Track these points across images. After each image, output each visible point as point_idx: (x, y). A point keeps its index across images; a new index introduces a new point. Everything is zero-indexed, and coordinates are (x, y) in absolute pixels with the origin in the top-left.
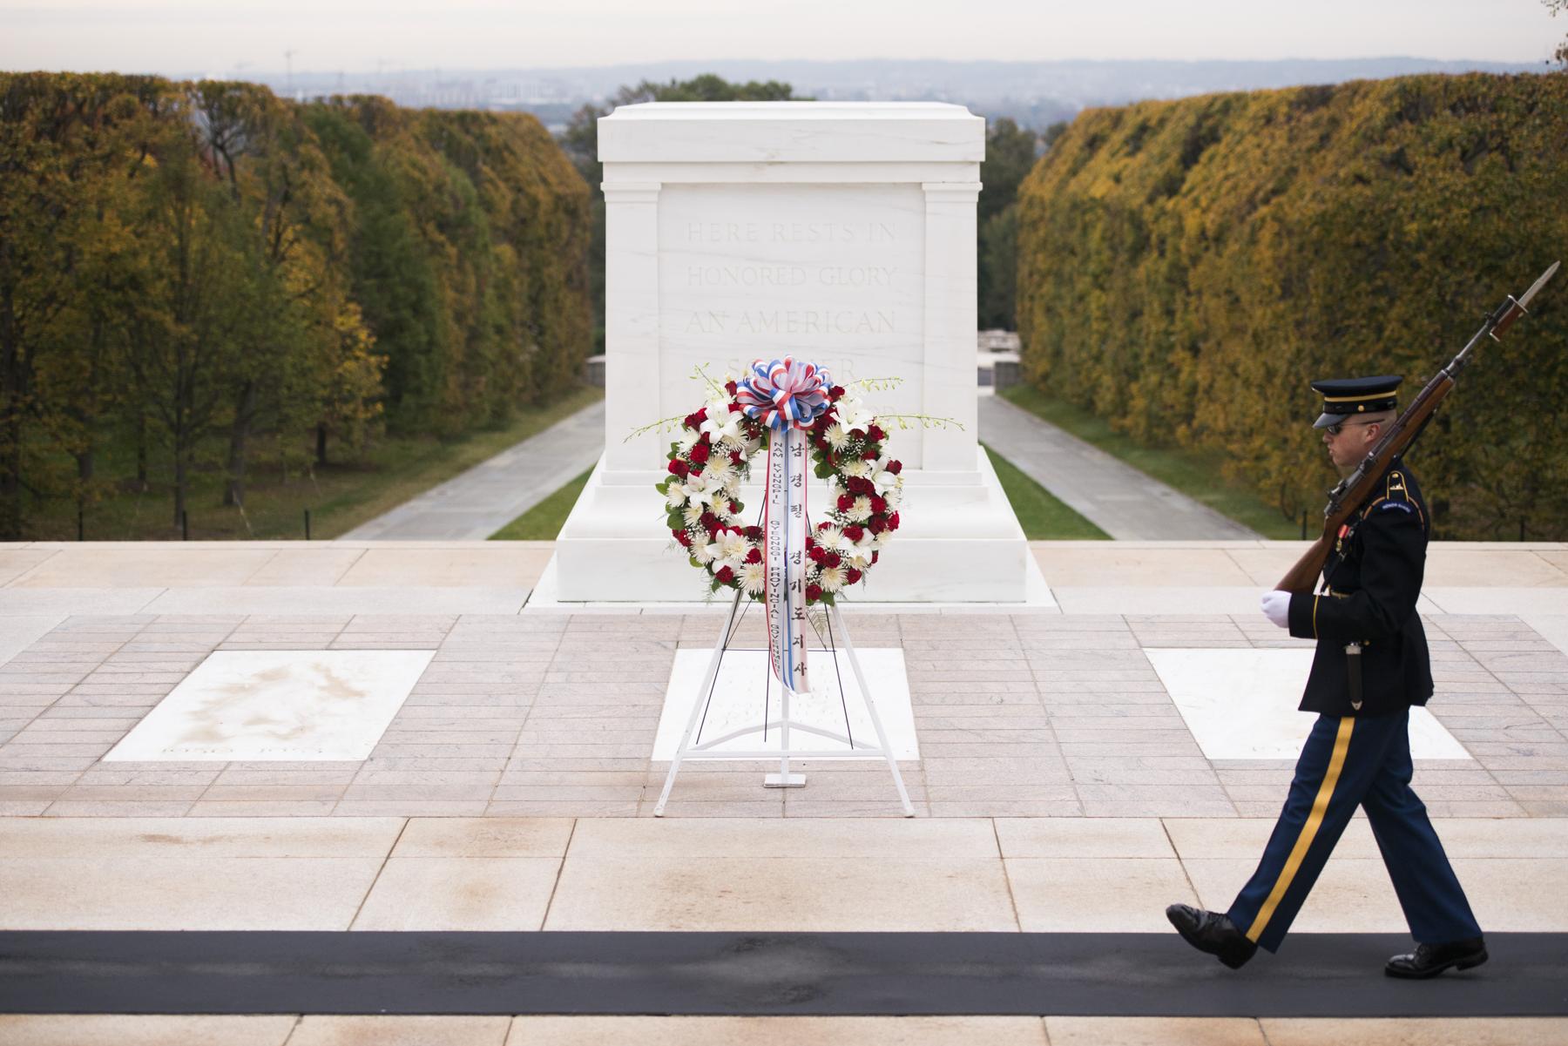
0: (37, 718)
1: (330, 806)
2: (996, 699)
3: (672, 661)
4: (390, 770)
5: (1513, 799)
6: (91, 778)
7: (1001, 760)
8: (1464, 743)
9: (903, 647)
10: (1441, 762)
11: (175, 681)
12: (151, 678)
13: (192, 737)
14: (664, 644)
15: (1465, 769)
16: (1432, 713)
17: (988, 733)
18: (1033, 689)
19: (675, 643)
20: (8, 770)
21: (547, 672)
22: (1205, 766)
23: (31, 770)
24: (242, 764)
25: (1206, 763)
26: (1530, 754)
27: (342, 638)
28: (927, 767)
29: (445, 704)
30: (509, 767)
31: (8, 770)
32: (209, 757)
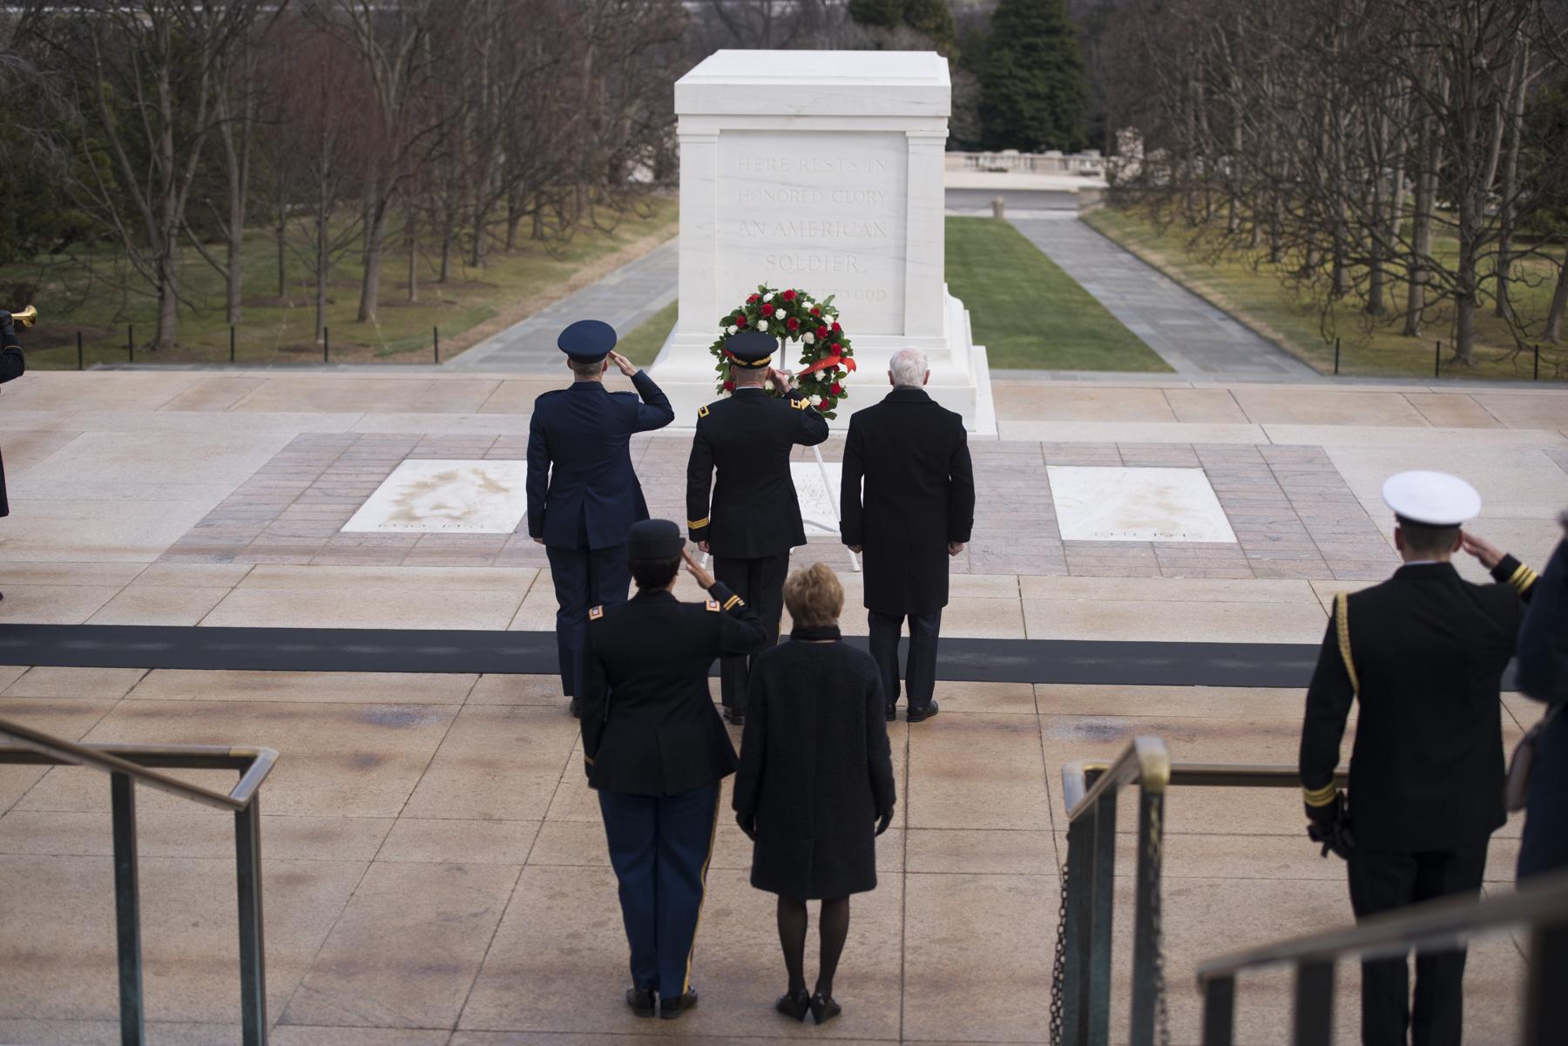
5: (1252, 568)
6: (335, 542)
10: (1216, 544)
11: (380, 479)
12: (364, 478)
13: (397, 517)
15: (1229, 547)
16: (1225, 512)
20: (280, 536)
22: (1059, 544)
24: (432, 534)
26: (1278, 539)
27: (491, 451)
31: (280, 536)
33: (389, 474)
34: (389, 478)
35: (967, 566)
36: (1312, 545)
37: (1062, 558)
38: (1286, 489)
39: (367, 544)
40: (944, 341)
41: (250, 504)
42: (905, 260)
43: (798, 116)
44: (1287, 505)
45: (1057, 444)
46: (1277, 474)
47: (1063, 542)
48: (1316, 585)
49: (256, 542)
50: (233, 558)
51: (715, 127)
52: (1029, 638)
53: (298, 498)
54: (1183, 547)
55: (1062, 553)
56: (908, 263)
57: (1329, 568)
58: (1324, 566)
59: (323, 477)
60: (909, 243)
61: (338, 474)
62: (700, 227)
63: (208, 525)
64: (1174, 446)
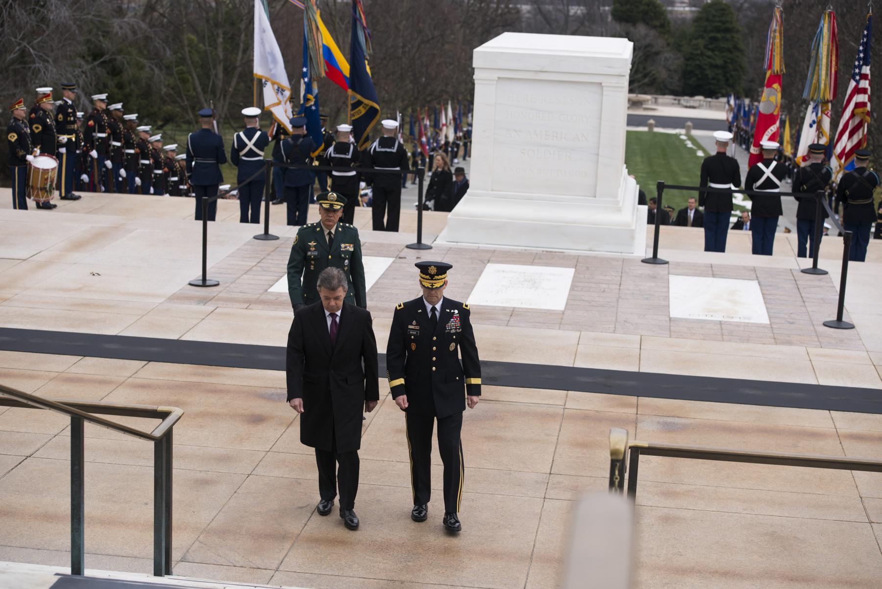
2: (602, 290)
3: (484, 268)
5: (775, 339)
6: (263, 297)
7: (593, 312)
8: (770, 318)
9: (576, 268)
10: (757, 324)
14: (483, 261)
17: (593, 302)
19: (487, 262)
20: (234, 292)
22: (668, 319)
26: (793, 323)
28: (565, 313)
29: (395, 279)
31: (234, 292)
35: (614, 329)
36: (812, 327)
37: (668, 327)
38: (803, 295)
41: (221, 273)
42: (598, 155)
44: (802, 304)
45: (678, 263)
46: (799, 287)
47: (670, 319)
48: (810, 350)
49: (220, 295)
50: (205, 304)
51: (496, 75)
52: (641, 371)
53: (248, 271)
54: (738, 325)
55: (668, 324)
57: (819, 341)
58: (816, 339)
59: (263, 261)
61: (272, 259)
64: (744, 268)
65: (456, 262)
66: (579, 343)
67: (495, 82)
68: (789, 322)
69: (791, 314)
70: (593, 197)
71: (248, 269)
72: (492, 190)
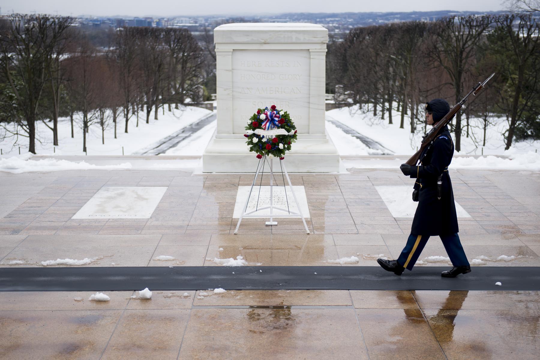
0: (51, 206)
1: (139, 232)
4: (157, 221)
5: (484, 229)
6: (68, 224)
8: (469, 212)
16: (459, 204)
18: (342, 197)
21: (201, 192)
23: (50, 221)
25: (393, 219)
30: (191, 220)
32: (103, 217)
33: (95, 193)
34: (96, 195)
35: (356, 230)
39: (83, 224)
40: (326, 136)
41: (32, 207)
42: (309, 103)
43: (265, 43)
47: (394, 218)
55: (396, 224)
56: (310, 104)
60: (311, 96)
62: (225, 90)
63: (10, 217)
65: (215, 186)
66: (336, 244)
67: (231, 53)
68: (485, 215)
69: (482, 208)
70: (307, 133)
71: (54, 202)
72: (233, 134)
